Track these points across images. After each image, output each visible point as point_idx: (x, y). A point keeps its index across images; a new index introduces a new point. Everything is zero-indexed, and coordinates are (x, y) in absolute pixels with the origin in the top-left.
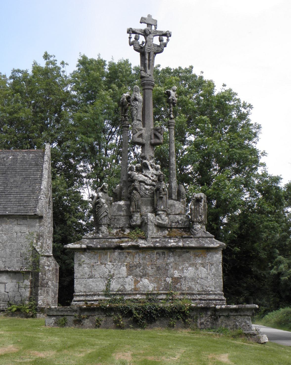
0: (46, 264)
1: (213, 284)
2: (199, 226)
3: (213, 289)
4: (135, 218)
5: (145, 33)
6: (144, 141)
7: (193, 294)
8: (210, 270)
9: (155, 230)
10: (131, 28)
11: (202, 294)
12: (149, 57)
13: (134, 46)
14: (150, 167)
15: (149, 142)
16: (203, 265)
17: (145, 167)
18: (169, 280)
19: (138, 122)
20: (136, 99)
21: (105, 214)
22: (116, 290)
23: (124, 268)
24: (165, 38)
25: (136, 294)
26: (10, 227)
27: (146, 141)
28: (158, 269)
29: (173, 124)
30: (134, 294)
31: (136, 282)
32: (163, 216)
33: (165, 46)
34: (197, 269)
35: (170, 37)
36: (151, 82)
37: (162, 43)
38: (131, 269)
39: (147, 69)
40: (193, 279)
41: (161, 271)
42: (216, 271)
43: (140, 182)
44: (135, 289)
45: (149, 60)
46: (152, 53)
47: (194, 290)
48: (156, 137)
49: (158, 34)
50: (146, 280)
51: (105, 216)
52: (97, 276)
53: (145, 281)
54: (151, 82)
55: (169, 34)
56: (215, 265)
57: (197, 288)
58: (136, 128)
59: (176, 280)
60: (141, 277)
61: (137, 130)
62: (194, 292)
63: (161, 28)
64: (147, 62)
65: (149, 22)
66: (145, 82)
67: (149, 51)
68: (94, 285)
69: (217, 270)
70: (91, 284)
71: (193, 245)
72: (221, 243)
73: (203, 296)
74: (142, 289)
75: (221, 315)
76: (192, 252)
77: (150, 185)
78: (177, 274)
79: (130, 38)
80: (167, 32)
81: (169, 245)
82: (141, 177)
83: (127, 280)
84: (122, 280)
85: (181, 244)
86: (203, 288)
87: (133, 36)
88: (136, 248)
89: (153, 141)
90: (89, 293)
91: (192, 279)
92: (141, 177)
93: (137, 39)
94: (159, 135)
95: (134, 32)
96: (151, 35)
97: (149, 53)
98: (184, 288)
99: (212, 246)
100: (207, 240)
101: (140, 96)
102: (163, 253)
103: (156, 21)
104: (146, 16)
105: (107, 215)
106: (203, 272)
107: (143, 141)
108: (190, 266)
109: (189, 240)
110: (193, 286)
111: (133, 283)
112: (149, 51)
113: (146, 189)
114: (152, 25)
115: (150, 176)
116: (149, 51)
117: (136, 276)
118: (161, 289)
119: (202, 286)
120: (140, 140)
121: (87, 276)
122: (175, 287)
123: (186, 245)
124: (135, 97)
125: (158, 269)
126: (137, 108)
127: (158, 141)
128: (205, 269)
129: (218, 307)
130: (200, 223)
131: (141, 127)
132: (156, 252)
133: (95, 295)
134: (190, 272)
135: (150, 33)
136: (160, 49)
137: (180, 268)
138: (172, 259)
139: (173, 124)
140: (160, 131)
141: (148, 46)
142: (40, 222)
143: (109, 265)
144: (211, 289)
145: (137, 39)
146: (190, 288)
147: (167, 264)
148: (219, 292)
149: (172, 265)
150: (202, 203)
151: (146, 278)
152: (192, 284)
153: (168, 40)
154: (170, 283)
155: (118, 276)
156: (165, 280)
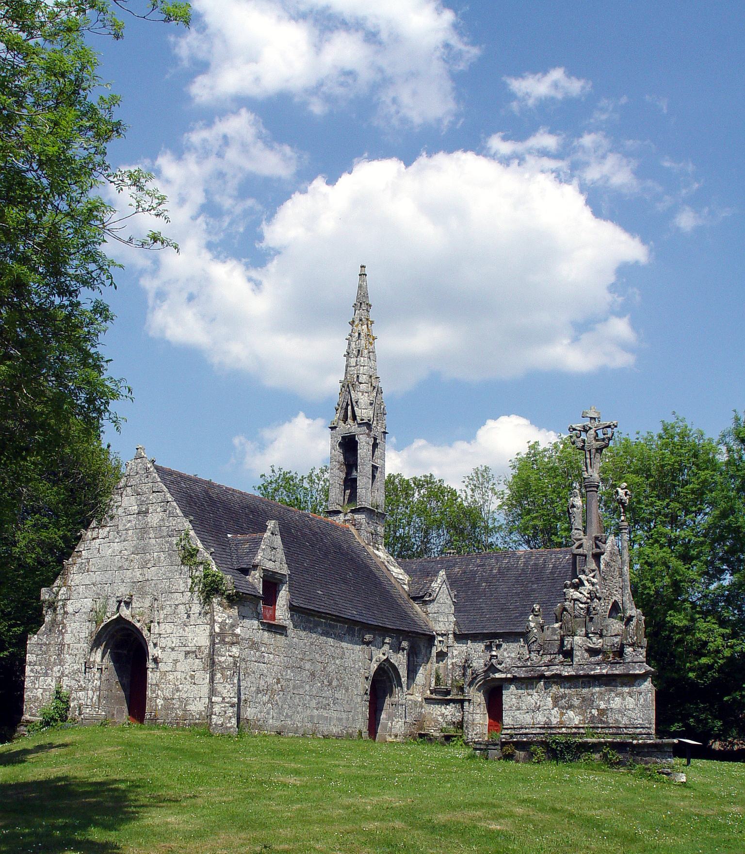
2: (631, 649)
4: (566, 642)
6: (586, 552)
9: (586, 655)
14: (586, 583)
16: (630, 694)
17: (581, 583)
18: (595, 712)
20: (573, 506)
23: (550, 699)
28: (584, 699)
31: (562, 714)
32: (594, 639)
33: (610, 439)
34: (624, 699)
38: (556, 700)
40: (620, 711)
41: (587, 702)
43: (575, 600)
44: (561, 722)
46: (593, 451)
47: (620, 722)
48: (597, 546)
53: (571, 713)
57: (624, 721)
59: (602, 712)
64: (588, 461)
68: (521, 717)
71: (617, 672)
72: (649, 668)
76: (619, 680)
77: (585, 603)
78: (603, 706)
81: (592, 673)
82: (575, 594)
83: (552, 712)
85: (604, 671)
92: (575, 594)
97: (590, 451)
99: (637, 672)
100: (637, 666)
101: (578, 501)
102: (589, 682)
106: (630, 702)
108: (616, 696)
109: (618, 666)
110: (620, 719)
111: (558, 715)
113: (582, 608)
114: (595, 418)
115: (585, 593)
117: (562, 708)
119: (630, 719)
120: (580, 551)
121: (514, 708)
123: (610, 672)
125: (584, 699)
127: (598, 550)
129: (635, 742)
130: (630, 646)
131: (582, 537)
134: (616, 703)
135: (590, 428)
138: (597, 689)
143: (536, 696)
146: (617, 721)
147: (592, 694)
150: (634, 623)
152: (618, 716)
156: (591, 712)
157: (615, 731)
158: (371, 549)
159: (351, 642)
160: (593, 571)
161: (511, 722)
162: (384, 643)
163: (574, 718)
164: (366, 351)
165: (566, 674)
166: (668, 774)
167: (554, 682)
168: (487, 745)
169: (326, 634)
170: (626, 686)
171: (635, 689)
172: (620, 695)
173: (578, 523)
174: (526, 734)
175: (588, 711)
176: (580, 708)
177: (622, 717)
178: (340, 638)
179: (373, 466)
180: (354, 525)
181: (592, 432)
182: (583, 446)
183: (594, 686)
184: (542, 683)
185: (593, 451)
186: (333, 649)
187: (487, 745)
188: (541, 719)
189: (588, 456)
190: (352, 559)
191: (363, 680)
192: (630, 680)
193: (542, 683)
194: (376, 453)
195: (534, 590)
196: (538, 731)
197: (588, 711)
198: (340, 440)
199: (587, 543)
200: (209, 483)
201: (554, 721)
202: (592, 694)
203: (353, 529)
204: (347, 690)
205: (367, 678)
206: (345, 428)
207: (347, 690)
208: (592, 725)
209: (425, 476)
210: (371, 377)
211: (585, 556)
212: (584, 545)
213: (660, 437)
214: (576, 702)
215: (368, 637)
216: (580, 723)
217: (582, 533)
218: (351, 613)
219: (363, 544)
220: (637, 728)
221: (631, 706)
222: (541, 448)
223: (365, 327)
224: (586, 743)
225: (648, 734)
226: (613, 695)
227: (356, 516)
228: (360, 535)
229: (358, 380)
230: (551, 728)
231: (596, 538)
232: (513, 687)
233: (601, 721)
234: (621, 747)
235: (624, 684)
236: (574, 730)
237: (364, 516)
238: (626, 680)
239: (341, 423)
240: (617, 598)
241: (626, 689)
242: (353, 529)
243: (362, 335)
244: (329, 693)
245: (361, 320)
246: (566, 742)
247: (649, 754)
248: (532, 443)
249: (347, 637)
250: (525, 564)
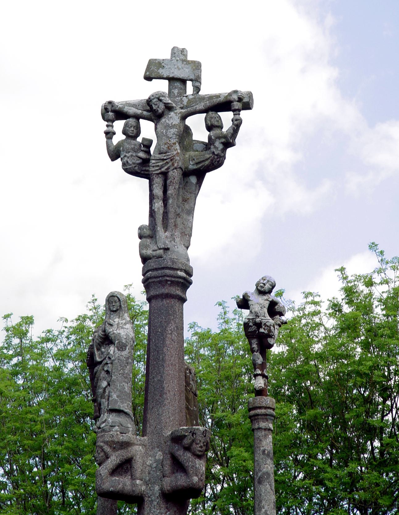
5: (154, 110)
6: (140, 486)
10: (110, 103)
12: (165, 191)
13: (122, 159)
15: (157, 488)
19: (111, 418)
24: (227, 118)
27: (146, 483)
29: (263, 411)
33: (229, 143)
35: (244, 114)
36: (168, 272)
37: (216, 132)
39: (160, 228)
45: (165, 200)
46: (175, 175)
48: (178, 466)
49: (201, 106)
54: (168, 272)
58: (106, 443)
61: (107, 449)
63: (213, 86)
65: (177, 72)
66: (148, 274)
67: (162, 167)
79: (109, 135)
80: (230, 94)
87: (119, 125)
89: (169, 483)
93: (132, 134)
94: (186, 457)
95: (120, 114)
96: (172, 114)
97: (165, 175)
103: (197, 66)
104: (165, 54)
107: (134, 485)
112: (163, 170)
116: (162, 167)
120: (123, 483)
124: (104, 331)
126: (109, 367)
127: (181, 480)
131: (130, 436)
135: (169, 108)
136: (212, 158)
139: (263, 411)
140: (186, 442)
141: (160, 153)
145: (132, 134)
173: (120, 392)
181: (173, 118)
182: (146, 162)
185: (175, 175)
189: (158, 191)
199: (146, 456)
212: (138, 465)
213: (336, 308)
217: (131, 426)
222: (35, 333)
231: (177, 439)
248: (15, 321)
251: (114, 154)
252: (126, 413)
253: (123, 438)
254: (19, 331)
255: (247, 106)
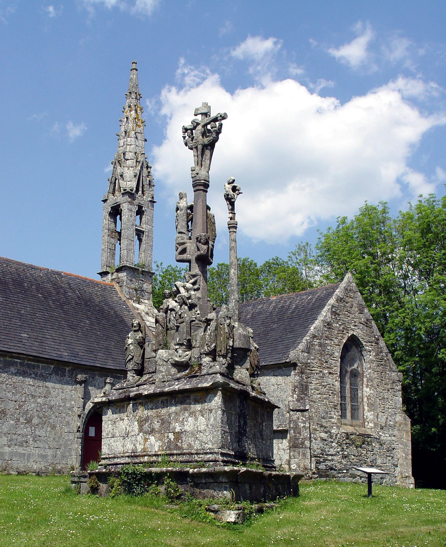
0: (300, 420)
1: (211, 439)
3: (210, 446)
7: (193, 454)
8: (209, 420)
9: (174, 370)
11: (200, 454)
18: (171, 436)
21: (130, 357)
22: (130, 451)
23: (136, 423)
24: (217, 123)
25: (145, 456)
26: (267, 380)
28: (163, 422)
30: (142, 456)
31: (146, 440)
34: (196, 419)
35: (223, 122)
42: (214, 420)
44: (144, 450)
50: (153, 437)
51: (130, 360)
52: (117, 434)
53: (152, 439)
55: (221, 116)
56: (214, 411)
57: (197, 446)
59: (178, 435)
60: (150, 434)
62: (193, 451)
69: (215, 419)
70: (113, 444)
73: (201, 456)
74: (150, 450)
75: (199, 482)
78: (178, 429)
79: (184, 137)
84: (134, 438)
85: (177, 388)
86: (201, 445)
88: (139, 397)
90: (110, 456)
91: (192, 433)
98: (185, 446)
105: (132, 359)
110: (193, 443)
111: (142, 442)
118: (165, 448)
122: (177, 445)
128: (204, 419)
132: (160, 399)
133: (114, 458)
134: (190, 424)
137: (181, 419)
138: (173, 409)
142: (295, 369)
144: (209, 446)
146: (190, 446)
148: (216, 450)
149: (173, 415)
151: (153, 435)
152: (191, 440)
153: (221, 125)
154: (172, 440)
155: (133, 433)
156: (168, 437)
157: (185, 458)
158: (132, 304)
159: (60, 382)
160: (194, 276)
161: (107, 452)
162: (106, 383)
163: (155, 444)
164: (133, 132)
165: (146, 393)
166: (216, 512)
167: (141, 404)
168: (79, 477)
169: (24, 374)
170: (199, 403)
171: (206, 405)
172: (192, 414)
174: (116, 464)
175: (166, 435)
176: (159, 432)
177: (195, 441)
178: (44, 378)
179: (136, 230)
180: (118, 283)
183: (171, 405)
184: (131, 405)
186: (32, 389)
187: (79, 477)
188: (129, 447)
190: (101, 311)
191: (76, 418)
192: (201, 395)
193: (131, 405)
194: (143, 219)
195: (273, 330)
196: (127, 460)
197: (166, 435)
198: (110, 210)
200: (7, 260)
201: (140, 448)
202: (169, 415)
203: (117, 287)
204: (53, 427)
205: (79, 416)
206: (112, 200)
207: (53, 427)
208: (168, 452)
209: (273, 259)
210: (136, 153)
211: (189, 261)
212: (188, 250)
214: (157, 426)
215: (80, 377)
216: (159, 450)
218: (66, 356)
219: (124, 299)
220: (206, 453)
221: (202, 428)
222: (348, 221)
223: (133, 112)
224: (151, 473)
225: (215, 461)
226: (187, 414)
227: (120, 275)
228: (122, 291)
229: (124, 158)
230: (136, 456)
232: (110, 412)
233: (177, 447)
234: (180, 477)
235: (197, 402)
236: (154, 458)
237: (125, 274)
238: (199, 395)
239: (111, 196)
240: (358, 332)
241: (198, 407)
242: (117, 287)
243: (130, 119)
244: (25, 430)
245: (130, 107)
246: (134, 473)
247: (207, 486)
249: (54, 377)
250: (275, 308)
251: (186, 144)
252: (184, 233)
253: (182, 241)
254: (343, 222)
255: (224, 118)
